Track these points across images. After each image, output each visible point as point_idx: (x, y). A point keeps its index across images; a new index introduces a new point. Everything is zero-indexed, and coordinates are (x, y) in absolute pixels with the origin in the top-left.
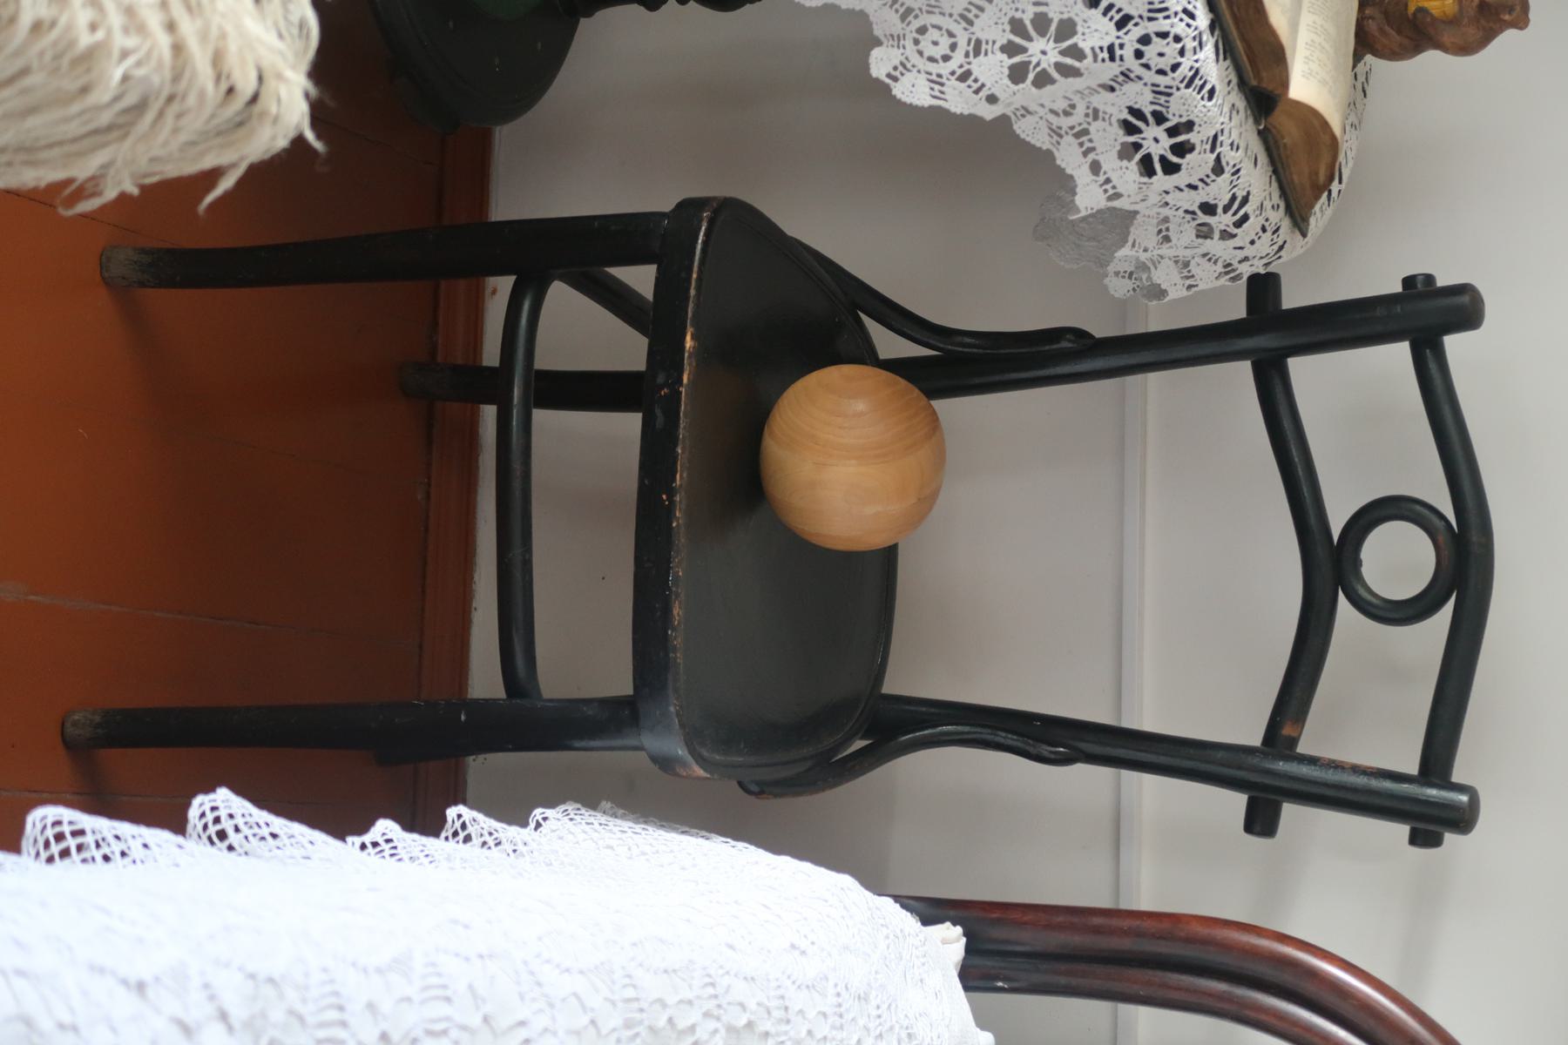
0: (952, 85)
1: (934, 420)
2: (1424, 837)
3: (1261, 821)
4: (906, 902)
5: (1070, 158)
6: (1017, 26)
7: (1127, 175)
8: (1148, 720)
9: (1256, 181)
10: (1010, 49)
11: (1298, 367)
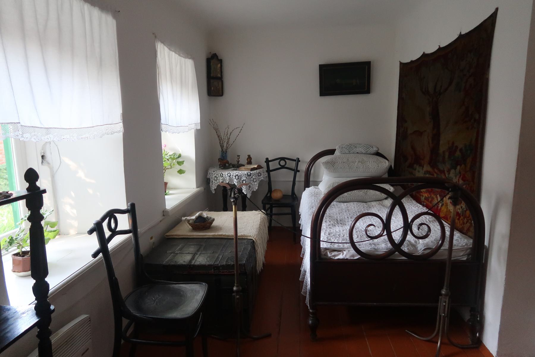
0: (257, 186)
1: (275, 190)
2: (299, 161)
3: (299, 171)
4: (304, 191)
5: (260, 180)
6: (253, 182)
7: (261, 176)
8: (292, 179)
9: (261, 170)
10: (255, 182)
11: (271, 169)
